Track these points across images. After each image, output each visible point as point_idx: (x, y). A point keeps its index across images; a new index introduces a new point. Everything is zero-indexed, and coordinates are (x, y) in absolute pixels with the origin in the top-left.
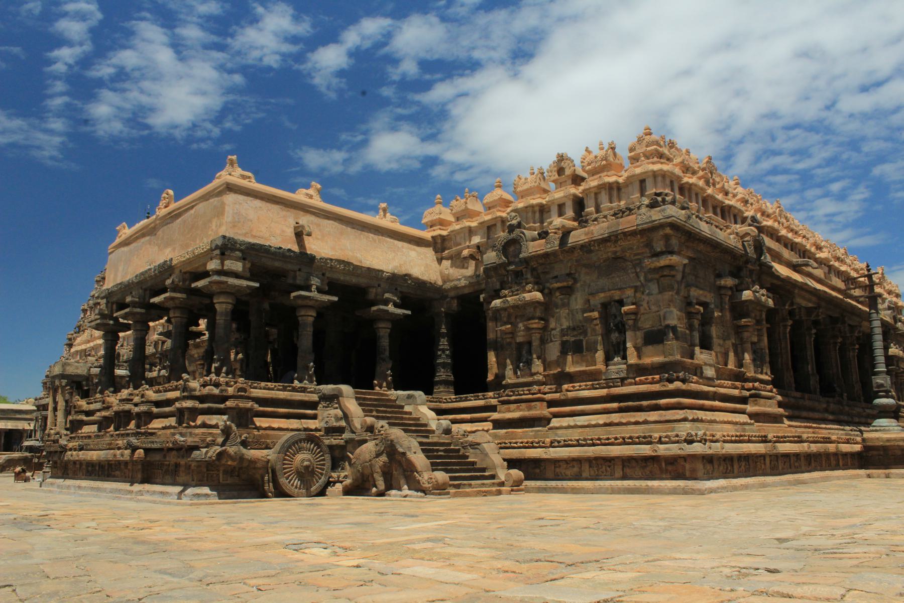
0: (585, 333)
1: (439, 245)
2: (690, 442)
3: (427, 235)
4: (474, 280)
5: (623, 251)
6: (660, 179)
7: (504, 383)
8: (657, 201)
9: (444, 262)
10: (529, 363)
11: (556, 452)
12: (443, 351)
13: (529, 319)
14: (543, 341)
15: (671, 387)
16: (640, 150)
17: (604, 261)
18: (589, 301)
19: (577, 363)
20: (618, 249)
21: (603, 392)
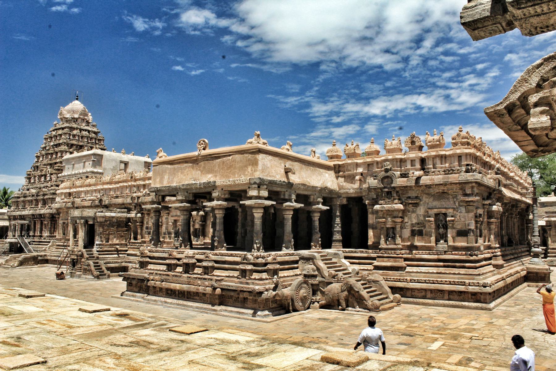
0: (425, 227)
1: (337, 169)
2: (485, 287)
3: (331, 163)
4: (359, 191)
5: (448, 190)
6: (468, 157)
7: (380, 247)
8: (469, 169)
9: (339, 178)
10: (394, 238)
11: (413, 285)
12: (338, 224)
13: (395, 217)
14: (402, 228)
15: (471, 258)
16: (459, 140)
17: (437, 193)
18: (428, 212)
19: (420, 240)
20: (445, 188)
21: (436, 257)
